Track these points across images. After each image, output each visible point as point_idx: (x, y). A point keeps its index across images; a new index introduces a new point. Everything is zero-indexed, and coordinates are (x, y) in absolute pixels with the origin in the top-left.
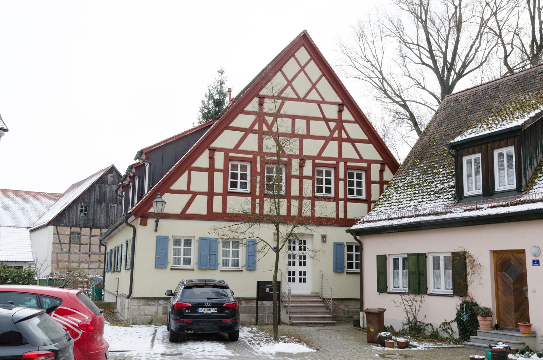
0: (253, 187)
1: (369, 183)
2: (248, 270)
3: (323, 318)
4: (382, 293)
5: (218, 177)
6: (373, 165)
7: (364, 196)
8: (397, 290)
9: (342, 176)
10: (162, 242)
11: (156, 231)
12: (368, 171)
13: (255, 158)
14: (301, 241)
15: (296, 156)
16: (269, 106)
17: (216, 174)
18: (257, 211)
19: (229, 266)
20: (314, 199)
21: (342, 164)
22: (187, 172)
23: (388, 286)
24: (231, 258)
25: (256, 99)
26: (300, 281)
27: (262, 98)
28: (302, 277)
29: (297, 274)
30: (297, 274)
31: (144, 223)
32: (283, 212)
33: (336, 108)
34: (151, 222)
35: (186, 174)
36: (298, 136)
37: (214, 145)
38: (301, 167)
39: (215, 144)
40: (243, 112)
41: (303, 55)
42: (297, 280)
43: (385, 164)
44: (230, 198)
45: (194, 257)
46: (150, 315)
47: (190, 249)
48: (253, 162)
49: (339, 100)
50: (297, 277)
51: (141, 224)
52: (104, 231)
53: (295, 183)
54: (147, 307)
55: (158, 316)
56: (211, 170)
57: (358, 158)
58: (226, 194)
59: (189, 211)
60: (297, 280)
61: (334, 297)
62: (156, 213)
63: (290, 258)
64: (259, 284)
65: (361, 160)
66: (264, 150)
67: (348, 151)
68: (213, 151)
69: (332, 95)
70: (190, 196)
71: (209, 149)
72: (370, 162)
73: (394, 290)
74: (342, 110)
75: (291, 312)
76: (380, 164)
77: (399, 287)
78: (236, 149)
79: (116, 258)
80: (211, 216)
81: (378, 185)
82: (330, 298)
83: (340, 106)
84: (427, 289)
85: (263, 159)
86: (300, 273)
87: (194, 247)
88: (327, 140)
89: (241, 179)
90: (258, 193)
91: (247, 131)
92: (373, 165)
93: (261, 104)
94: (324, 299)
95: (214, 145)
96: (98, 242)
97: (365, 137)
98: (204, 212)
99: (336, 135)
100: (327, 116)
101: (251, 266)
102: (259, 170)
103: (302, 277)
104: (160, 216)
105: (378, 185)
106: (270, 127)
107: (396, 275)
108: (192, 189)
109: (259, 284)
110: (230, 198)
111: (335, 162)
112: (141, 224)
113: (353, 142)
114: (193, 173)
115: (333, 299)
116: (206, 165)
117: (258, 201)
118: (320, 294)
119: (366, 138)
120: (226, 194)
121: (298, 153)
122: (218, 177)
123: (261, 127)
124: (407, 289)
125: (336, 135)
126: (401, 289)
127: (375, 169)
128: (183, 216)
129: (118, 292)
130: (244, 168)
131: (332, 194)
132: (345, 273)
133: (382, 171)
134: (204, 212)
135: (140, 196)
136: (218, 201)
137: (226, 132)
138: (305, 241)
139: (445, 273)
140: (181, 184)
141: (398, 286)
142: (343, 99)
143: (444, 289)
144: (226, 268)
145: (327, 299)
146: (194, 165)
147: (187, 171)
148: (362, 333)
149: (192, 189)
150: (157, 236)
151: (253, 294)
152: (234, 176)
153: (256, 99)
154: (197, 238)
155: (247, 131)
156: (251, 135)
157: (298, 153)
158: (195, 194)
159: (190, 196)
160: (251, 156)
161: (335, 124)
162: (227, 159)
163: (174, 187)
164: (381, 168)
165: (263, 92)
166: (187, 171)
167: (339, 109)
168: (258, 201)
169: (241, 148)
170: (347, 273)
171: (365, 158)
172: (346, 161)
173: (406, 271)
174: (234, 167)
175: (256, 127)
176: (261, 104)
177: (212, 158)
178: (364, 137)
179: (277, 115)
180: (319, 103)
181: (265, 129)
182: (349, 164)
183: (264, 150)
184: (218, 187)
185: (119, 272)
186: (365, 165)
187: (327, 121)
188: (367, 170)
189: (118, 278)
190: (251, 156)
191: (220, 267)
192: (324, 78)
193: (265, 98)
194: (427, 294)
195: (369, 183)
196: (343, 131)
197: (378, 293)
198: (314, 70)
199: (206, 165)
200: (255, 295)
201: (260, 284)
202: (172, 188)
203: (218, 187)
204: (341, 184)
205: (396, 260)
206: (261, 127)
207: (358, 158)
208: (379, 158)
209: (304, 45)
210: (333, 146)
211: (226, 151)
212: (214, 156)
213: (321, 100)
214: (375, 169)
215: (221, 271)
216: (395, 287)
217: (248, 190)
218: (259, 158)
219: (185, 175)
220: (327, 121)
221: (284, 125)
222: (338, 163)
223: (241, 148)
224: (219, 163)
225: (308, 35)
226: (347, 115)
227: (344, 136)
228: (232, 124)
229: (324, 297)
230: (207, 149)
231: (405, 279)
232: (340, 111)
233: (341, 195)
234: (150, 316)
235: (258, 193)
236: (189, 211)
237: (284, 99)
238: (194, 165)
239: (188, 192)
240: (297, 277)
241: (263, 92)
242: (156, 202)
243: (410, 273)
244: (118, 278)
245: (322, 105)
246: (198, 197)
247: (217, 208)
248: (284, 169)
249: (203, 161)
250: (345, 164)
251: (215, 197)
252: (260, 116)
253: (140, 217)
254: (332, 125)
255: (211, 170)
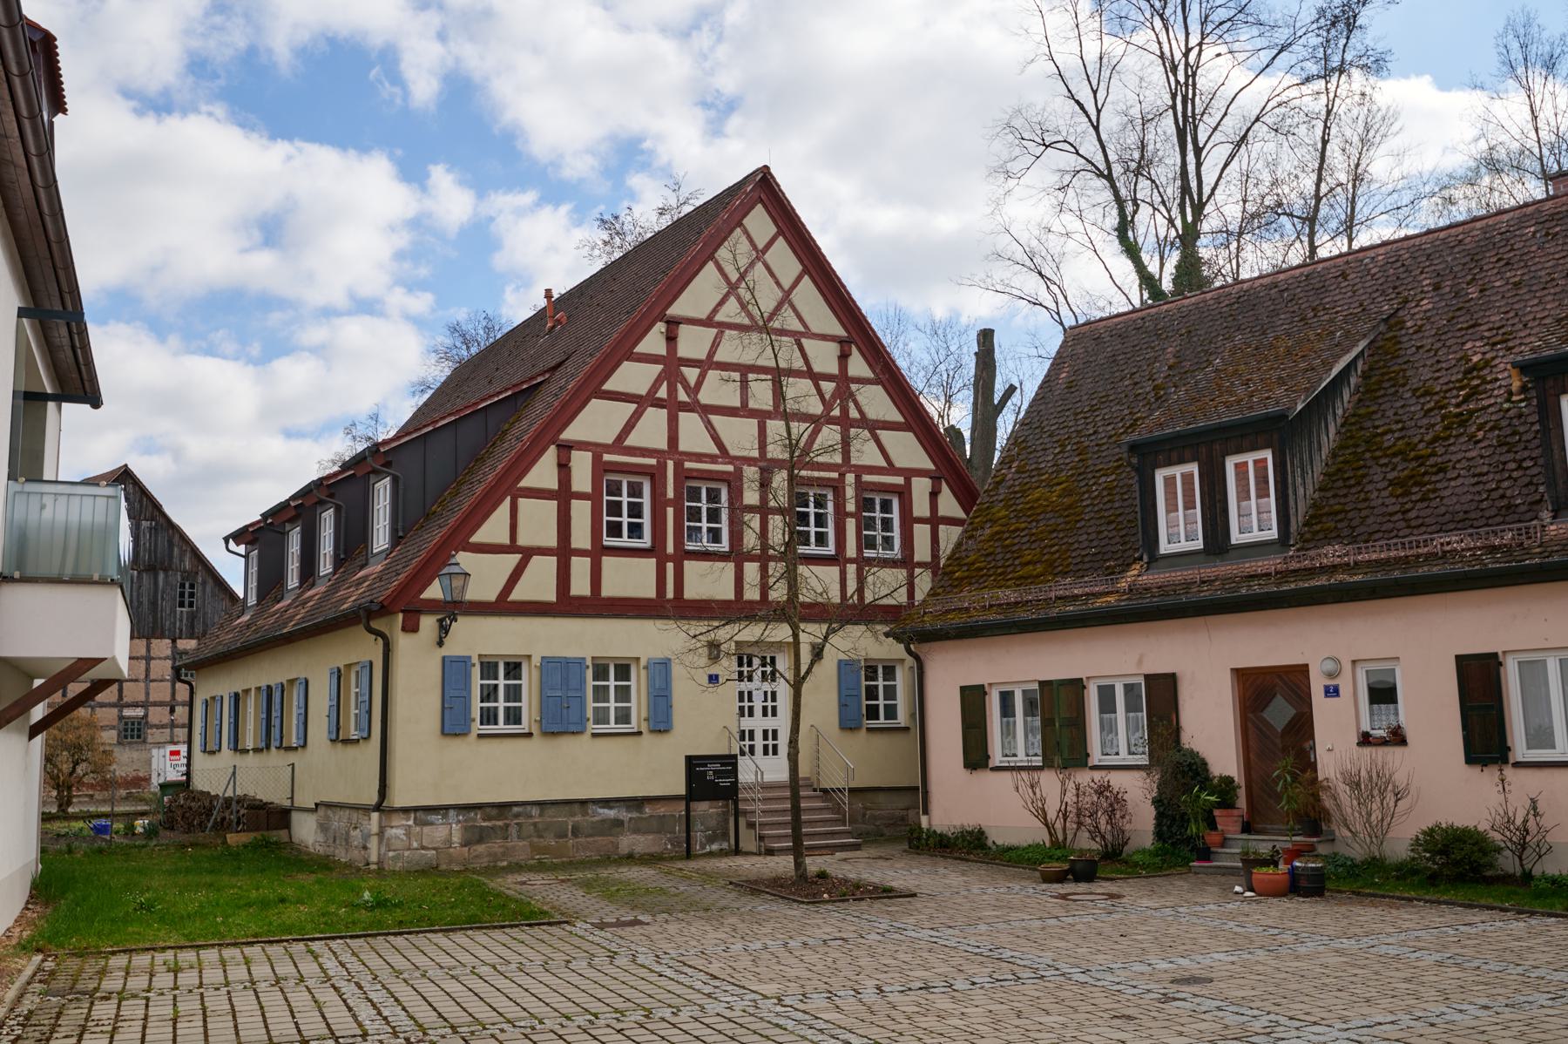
0: (736, 537)
1: (908, 520)
2: (652, 731)
3: (833, 834)
4: (975, 769)
5: (581, 512)
6: (915, 481)
7: (897, 551)
8: (1012, 761)
9: (851, 507)
10: (454, 670)
11: (440, 643)
12: (904, 493)
13: (662, 467)
14: (765, 658)
15: (749, 461)
16: (692, 343)
17: (576, 504)
18: (670, 594)
19: (496, 724)
20: (862, 562)
21: (850, 478)
22: (508, 501)
23: (990, 753)
24: (612, 705)
25: (660, 327)
26: (766, 752)
27: (673, 324)
28: (770, 742)
29: (759, 736)
30: (759, 736)
31: (411, 627)
32: (778, 593)
33: (833, 349)
34: (428, 623)
35: (506, 505)
36: (753, 413)
37: (569, 434)
38: (764, 485)
39: (570, 434)
40: (632, 357)
41: (759, 223)
42: (759, 749)
43: (940, 478)
44: (608, 562)
45: (528, 706)
46: (434, 849)
47: (629, 687)
48: (656, 475)
49: (840, 331)
50: (759, 742)
51: (404, 629)
52: (188, 644)
53: (921, 533)
54: (426, 829)
55: (451, 850)
56: (563, 495)
57: (884, 464)
58: (598, 552)
59: (517, 595)
60: (759, 749)
61: (853, 785)
62: (449, 602)
63: (741, 699)
64: (691, 761)
65: (891, 469)
66: (683, 447)
67: (866, 453)
68: (566, 448)
69: (823, 319)
70: (515, 559)
71: (558, 446)
72: (908, 474)
73: (1003, 762)
74: (848, 353)
75: (762, 825)
76: (931, 478)
77: (1117, 754)
78: (618, 445)
79: (275, 714)
80: (566, 606)
81: (928, 527)
82: (844, 789)
83: (844, 344)
84: (1088, 755)
85: (678, 466)
86: (765, 732)
87: (528, 681)
88: (817, 422)
89: (816, 526)
90: (670, 549)
91: (643, 402)
92: (915, 481)
93: (671, 339)
94: (825, 791)
95: (569, 434)
96: (168, 675)
97: (897, 417)
98: (551, 596)
99: (836, 412)
100: (817, 368)
101: (661, 724)
102: (670, 494)
103: (770, 742)
104: (452, 610)
105: (928, 527)
106: (694, 390)
107: (1008, 731)
108: (522, 541)
109: (691, 761)
110: (608, 562)
111: (835, 475)
112: (404, 629)
113: (874, 426)
114: (523, 503)
115: (852, 791)
116: (552, 483)
117: (670, 566)
118: (814, 779)
119: (900, 419)
120: (598, 552)
121: (755, 454)
122: (581, 512)
123: (672, 391)
124: (1040, 758)
125: (836, 412)
126: (1021, 758)
127: (921, 487)
128: (503, 606)
129: (292, 798)
130: (635, 491)
131: (831, 549)
132: (864, 730)
133: (934, 494)
134: (551, 596)
135: (342, 556)
136: (580, 569)
137: (595, 403)
138: (773, 659)
139: (1127, 719)
140: (494, 529)
141: (1115, 751)
142: (850, 327)
143: (1126, 752)
144: (601, 728)
145: (834, 791)
146: (524, 483)
147: (509, 499)
148: (892, 866)
149: (522, 541)
150: (444, 658)
151: (676, 784)
152: (615, 508)
153: (660, 327)
154: (536, 661)
155: (643, 402)
156: (651, 412)
157: (755, 454)
158: (528, 553)
159: (515, 559)
160: (653, 461)
161: (833, 385)
162: (600, 468)
163: (478, 537)
164: (933, 487)
165: (675, 310)
166: (509, 499)
167: (842, 350)
168: (670, 566)
169: (629, 442)
170: (869, 730)
171: (898, 464)
172: (860, 470)
173: (1037, 722)
174: (615, 489)
175: (662, 393)
176: (671, 339)
177: (564, 467)
178: (895, 415)
179: (707, 364)
180: (797, 337)
181: (682, 396)
182: (867, 478)
183: (683, 447)
184: (581, 537)
185: (212, 753)
186: (900, 480)
187: (816, 378)
188: (903, 493)
189: (293, 764)
190: (653, 461)
191: (477, 727)
192: (806, 279)
193: (680, 323)
194: (1086, 765)
195: (908, 520)
196: (851, 405)
197: (965, 773)
198: (784, 260)
199: (552, 483)
200: (681, 790)
201: (694, 764)
202: (475, 539)
203: (581, 537)
204: (851, 524)
205: (1007, 698)
206: (672, 391)
207: (884, 464)
208: (928, 464)
209: (762, 201)
210: (830, 435)
211: (597, 449)
212: (570, 461)
213: (802, 329)
214: (921, 487)
215: (595, 735)
216: (1007, 756)
217: (831, 549)
218: (670, 464)
219: (505, 508)
220: (816, 378)
221: (716, 390)
222: (842, 475)
223: (629, 442)
224: (582, 480)
225: (773, 177)
226: (858, 366)
227: (854, 414)
228: (609, 386)
229: (825, 785)
230: (553, 443)
231: (1133, 735)
232: (844, 357)
233: (851, 551)
234: (434, 852)
235: (670, 549)
236: (517, 595)
237: (723, 326)
238: (524, 483)
239: (512, 548)
240: (759, 742)
241: (675, 310)
242: (450, 574)
243: (1047, 724)
244: (293, 764)
245: (804, 341)
246: (535, 559)
247: (580, 586)
248: (830, 497)
249: (543, 473)
250: (858, 478)
251: (574, 559)
252: (672, 365)
253: (402, 611)
254: (828, 387)
255: (563, 495)
